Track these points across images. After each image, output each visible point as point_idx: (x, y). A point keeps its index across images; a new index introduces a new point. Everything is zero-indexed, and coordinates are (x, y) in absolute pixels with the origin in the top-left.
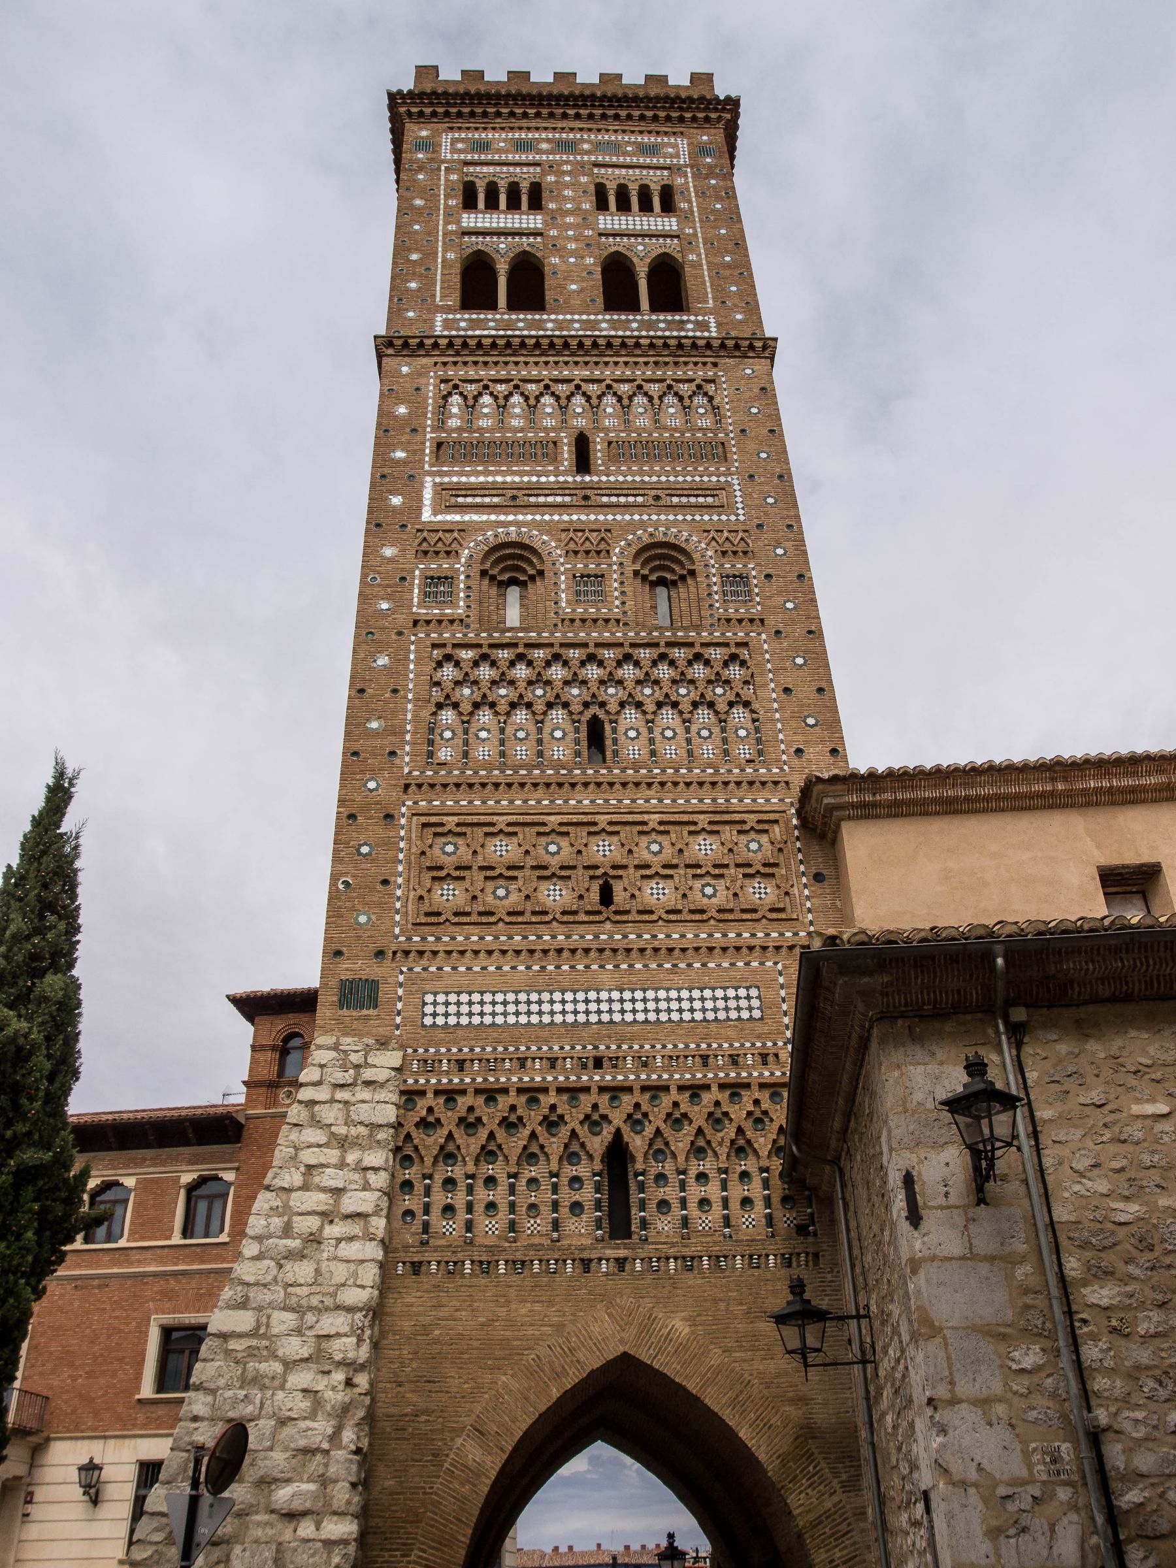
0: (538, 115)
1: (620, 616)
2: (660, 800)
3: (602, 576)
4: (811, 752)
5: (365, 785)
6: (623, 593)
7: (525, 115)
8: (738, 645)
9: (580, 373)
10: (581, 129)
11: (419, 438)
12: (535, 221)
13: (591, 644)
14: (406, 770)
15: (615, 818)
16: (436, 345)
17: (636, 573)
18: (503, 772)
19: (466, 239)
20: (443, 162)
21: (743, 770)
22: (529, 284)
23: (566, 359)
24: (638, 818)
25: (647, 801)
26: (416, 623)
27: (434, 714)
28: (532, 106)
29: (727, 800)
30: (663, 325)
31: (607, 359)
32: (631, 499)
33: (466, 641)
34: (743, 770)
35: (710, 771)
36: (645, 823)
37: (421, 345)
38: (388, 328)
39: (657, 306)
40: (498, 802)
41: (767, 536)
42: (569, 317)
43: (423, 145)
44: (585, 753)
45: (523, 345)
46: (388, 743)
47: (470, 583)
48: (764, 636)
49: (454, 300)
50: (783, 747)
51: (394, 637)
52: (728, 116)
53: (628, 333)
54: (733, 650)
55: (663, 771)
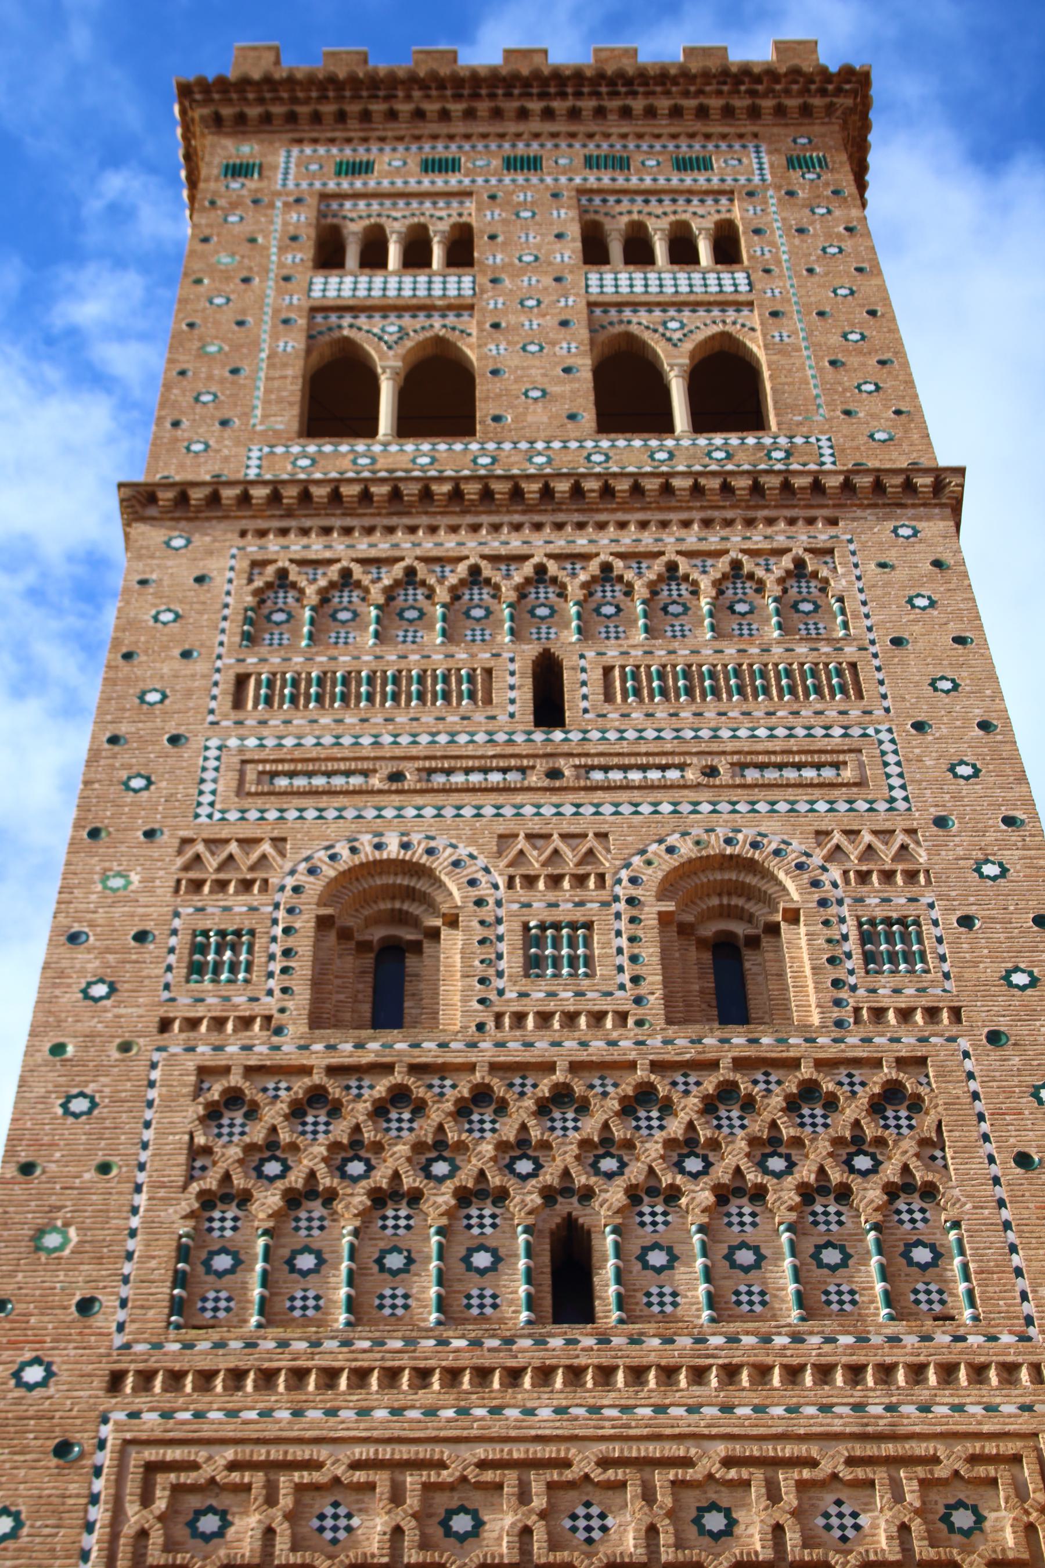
0: (470, 114)
1: (629, 1006)
2: (727, 1409)
3: (589, 926)
9: (540, 545)
11: (199, 666)
12: (459, 285)
13: (562, 1065)
14: (119, 1340)
15: (616, 1450)
16: (245, 499)
17: (664, 919)
19: (319, 318)
20: (278, 194)
22: (443, 393)
23: (517, 518)
26: (165, 1025)
27: (191, 1215)
28: (458, 97)
30: (725, 450)
31: (602, 517)
32: (654, 775)
33: (278, 1059)
36: (687, 1462)
37: (214, 499)
38: (148, 471)
41: (960, 843)
42: (523, 445)
44: (547, 1302)
47: (290, 942)
48: (964, 1044)
49: (288, 419)
51: (116, 1055)
52: (849, 102)
55: (733, 1340)
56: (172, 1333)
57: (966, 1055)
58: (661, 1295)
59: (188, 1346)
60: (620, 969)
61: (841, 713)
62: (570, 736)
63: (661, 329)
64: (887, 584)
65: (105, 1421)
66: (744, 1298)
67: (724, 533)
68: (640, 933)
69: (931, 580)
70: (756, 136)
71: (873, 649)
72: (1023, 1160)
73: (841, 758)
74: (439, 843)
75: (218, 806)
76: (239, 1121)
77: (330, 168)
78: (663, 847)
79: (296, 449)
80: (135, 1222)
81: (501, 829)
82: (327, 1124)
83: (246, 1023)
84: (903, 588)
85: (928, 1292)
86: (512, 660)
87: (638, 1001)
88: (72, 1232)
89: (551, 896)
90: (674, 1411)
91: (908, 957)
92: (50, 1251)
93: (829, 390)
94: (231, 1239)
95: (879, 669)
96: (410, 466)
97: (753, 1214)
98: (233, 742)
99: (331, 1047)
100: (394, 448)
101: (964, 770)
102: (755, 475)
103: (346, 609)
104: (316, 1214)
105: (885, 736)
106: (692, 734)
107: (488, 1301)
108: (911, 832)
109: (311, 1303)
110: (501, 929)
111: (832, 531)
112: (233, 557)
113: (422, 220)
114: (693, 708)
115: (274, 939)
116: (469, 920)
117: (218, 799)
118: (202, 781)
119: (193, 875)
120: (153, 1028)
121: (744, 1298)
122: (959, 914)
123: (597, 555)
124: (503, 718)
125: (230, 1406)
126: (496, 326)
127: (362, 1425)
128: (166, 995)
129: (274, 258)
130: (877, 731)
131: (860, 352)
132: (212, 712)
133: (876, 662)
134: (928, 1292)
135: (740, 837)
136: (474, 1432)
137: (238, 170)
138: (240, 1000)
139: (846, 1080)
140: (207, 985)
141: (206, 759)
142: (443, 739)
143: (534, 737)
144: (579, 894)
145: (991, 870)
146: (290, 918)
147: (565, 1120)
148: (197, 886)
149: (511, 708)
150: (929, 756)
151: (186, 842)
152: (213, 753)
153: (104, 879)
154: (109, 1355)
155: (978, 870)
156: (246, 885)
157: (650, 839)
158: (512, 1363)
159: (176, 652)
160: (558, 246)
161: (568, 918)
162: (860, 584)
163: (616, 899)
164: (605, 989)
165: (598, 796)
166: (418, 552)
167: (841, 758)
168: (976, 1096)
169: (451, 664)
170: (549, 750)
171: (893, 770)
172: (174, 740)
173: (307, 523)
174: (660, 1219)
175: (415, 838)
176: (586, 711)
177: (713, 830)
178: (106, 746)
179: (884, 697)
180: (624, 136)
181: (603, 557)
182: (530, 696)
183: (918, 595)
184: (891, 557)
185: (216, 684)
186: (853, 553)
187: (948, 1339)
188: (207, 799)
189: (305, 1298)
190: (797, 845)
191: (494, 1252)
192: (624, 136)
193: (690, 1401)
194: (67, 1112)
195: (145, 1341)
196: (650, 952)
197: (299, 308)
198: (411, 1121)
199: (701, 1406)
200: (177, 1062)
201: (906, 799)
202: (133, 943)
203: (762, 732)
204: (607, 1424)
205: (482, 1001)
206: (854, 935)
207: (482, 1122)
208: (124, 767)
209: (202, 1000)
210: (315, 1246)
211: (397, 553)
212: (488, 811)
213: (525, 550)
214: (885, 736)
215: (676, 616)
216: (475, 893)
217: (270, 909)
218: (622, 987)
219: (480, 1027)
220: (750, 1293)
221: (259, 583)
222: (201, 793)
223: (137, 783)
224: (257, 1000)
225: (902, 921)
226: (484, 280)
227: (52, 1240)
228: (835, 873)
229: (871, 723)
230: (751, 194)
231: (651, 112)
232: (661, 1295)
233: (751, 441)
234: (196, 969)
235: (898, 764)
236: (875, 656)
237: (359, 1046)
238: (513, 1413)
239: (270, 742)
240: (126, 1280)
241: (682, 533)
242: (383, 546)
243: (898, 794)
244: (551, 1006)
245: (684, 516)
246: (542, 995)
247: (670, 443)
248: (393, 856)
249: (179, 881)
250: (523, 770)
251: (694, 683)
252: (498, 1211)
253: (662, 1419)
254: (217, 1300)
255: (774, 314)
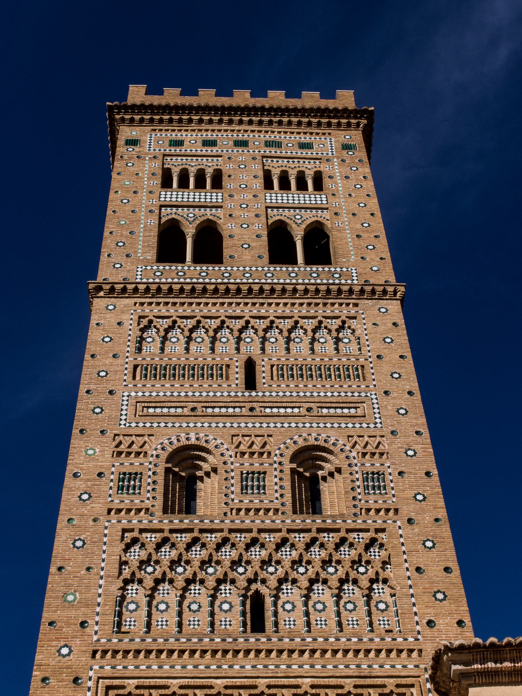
1: (279, 506)
2: (312, 666)
3: (265, 473)
4: (441, 623)
5: (59, 651)
6: (281, 487)
7: (211, 122)
8: (377, 531)
9: (247, 312)
10: (253, 131)
11: (120, 361)
13: (255, 530)
14: (95, 638)
15: (273, 682)
16: (136, 290)
18: (177, 640)
21: (383, 639)
22: (210, 245)
24: (293, 681)
25: (301, 666)
26: (109, 511)
29: (370, 666)
32: (289, 410)
34: (383, 639)
35: (355, 640)
37: (124, 290)
39: (308, 261)
40: (172, 667)
41: (400, 441)
42: (241, 269)
43: (132, 142)
45: (205, 290)
46: (80, 614)
47: (155, 478)
48: (399, 523)
49: (152, 255)
50: (416, 618)
51: (91, 523)
53: (288, 281)
54: (374, 535)
55: (315, 639)
56: (115, 635)
57: (400, 528)
58: (290, 621)
59: (121, 640)
60: (276, 491)
61: (358, 386)
62: (258, 394)
63: (293, 219)
64: (376, 332)
65: (91, 669)
66: (319, 622)
67: (316, 309)
68: (283, 477)
69: (393, 331)
70: (330, 134)
71: (370, 360)
72: (418, 569)
73: (357, 405)
74: (211, 437)
75: (128, 421)
76: (137, 550)
77: (167, 143)
78: (292, 441)
79: (155, 268)
80: (100, 591)
81: (233, 432)
82: (170, 552)
83: (139, 511)
84: (381, 334)
85: (384, 621)
86: (237, 361)
87: (283, 504)
88: (77, 594)
89: (251, 461)
90: (294, 667)
91: (379, 487)
92: (70, 602)
93: (356, 248)
94: (135, 598)
95: (372, 368)
96: (198, 276)
97: (323, 590)
98: (133, 394)
99: (171, 521)
100: (192, 268)
101: (402, 411)
102: (328, 284)
103: (174, 337)
104: (166, 588)
105: (374, 397)
106: (303, 394)
107: (228, 623)
108: (382, 436)
109: (164, 623)
110: (233, 474)
111: (356, 309)
112: (132, 314)
113: (203, 167)
114: (303, 383)
115: (149, 477)
116: (221, 471)
117: (128, 418)
118: (122, 410)
119: (118, 449)
120: (106, 512)
121: (319, 622)
122: (399, 470)
123: (269, 317)
124: (234, 386)
125: (136, 664)
126: (230, 215)
127: (183, 672)
128: (110, 499)
129: (146, 183)
130: (371, 394)
131: (367, 231)
132: (125, 380)
133: (371, 365)
134: (384, 621)
135: (320, 437)
136: (223, 675)
137: (132, 142)
138: (137, 501)
139: (357, 537)
140: (125, 495)
141: (123, 400)
142: (211, 394)
143: (245, 394)
144: (261, 460)
145: (411, 453)
146: (155, 468)
147: (256, 551)
148: (120, 454)
149: (237, 382)
150: (389, 405)
151: (116, 435)
152: (125, 398)
153: (86, 451)
154: (92, 643)
155: (406, 453)
156: (138, 454)
157: (287, 436)
158: (236, 648)
159: (111, 355)
160: (254, 181)
161: (257, 470)
162: (366, 332)
163: (275, 462)
164: (271, 499)
165: (268, 419)
166: (202, 314)
167: (357, 405)
168: (403, 544)
169: (214, 362)
170: (250, 400)
171: (376, 411)
172: (111, 392)
173: (160, 300)
174: (289, 591)
175: (201, 435)
176: (264, 383)
177: (310, 435)
178: (86, 394)
179: (374, 380)
180: (279, 132)
181: (272, 318)
182: (243, 376)
183: (387, 337)
184: (378, 321)
185: (126, 369)
186: (364, 319)
187: (390, 639)
188: (123, 417)
189: (162, 621)
190: (341, 442)
191: (230, 603)
192: (279, 132)
193: (299, 663)
194: (74, 546)
195: (105, 638)
196: (287, 484)
197: (156, 205)
198: (200, 551)
199: (303, 665)
200: (114, 525)
201: (381, 423)
202: (97, 478)
203: (329, 394)
204: (270, 671)
205: (226, 503)
206: (361, 479)
207: (226, 552)
208: (93, 403)
209: (123, 501)
210: (166, 600)
211: (194, 314)
212: (228, 425)
213: (242, 314)
214: (374, 397)
215: (298, 343)
216: (223, 459)
217: (148, 464)
218: (277, 498)
219: (225, 514)
220: (321, 621)
221: (142, 326)
222: (121, 415)
223: (98, 410)
224: (144, 501)
225: (378, 473)
226: (226, 195)
227: (70, 598)
228: (354, 454)
229: (369, 391)
230: (327, 160)
231: (290, 123)
232: (290, 621)
233: (326, 269)
234: (121, 488)
235: (378, 408)
236: (371, 362)
237: (181, 521)
238: (237, 667)
239: (147, 394)
240: (98, 614)
241: (300, 308)
242: (189, 312)
243: (378, 420)
244: (251, 506)
245: (301, 301)
246: (248, 501)
247: (296, 269)
248: (193, 443)
249: (114, 452)
250: (241, 407)
251: (304, 372)
252: (232, 588)
253: (289, 670)
254: (130, 621)
255: (336, 214)
